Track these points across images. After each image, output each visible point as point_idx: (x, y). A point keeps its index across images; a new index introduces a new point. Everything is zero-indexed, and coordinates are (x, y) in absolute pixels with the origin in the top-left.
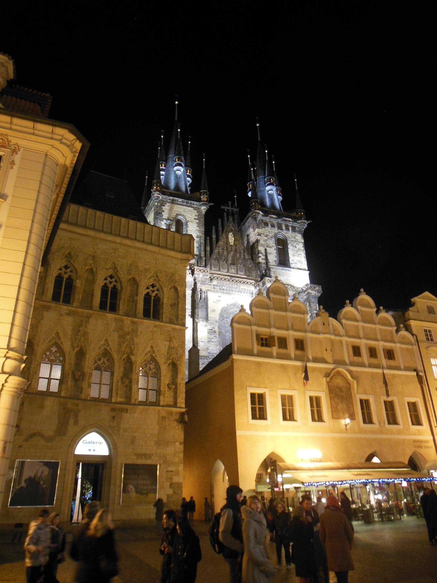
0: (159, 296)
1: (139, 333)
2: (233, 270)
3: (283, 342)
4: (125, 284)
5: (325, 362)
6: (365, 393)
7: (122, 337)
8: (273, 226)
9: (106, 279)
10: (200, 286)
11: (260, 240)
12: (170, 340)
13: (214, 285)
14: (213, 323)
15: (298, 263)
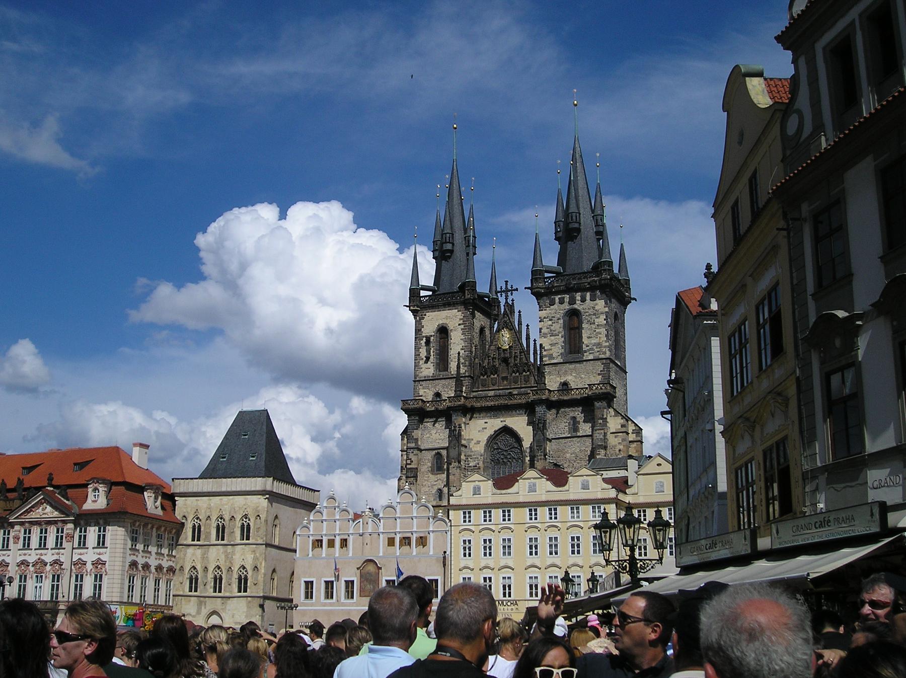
3: (331, 543)
7: (227, 556)
8: (562, 302)
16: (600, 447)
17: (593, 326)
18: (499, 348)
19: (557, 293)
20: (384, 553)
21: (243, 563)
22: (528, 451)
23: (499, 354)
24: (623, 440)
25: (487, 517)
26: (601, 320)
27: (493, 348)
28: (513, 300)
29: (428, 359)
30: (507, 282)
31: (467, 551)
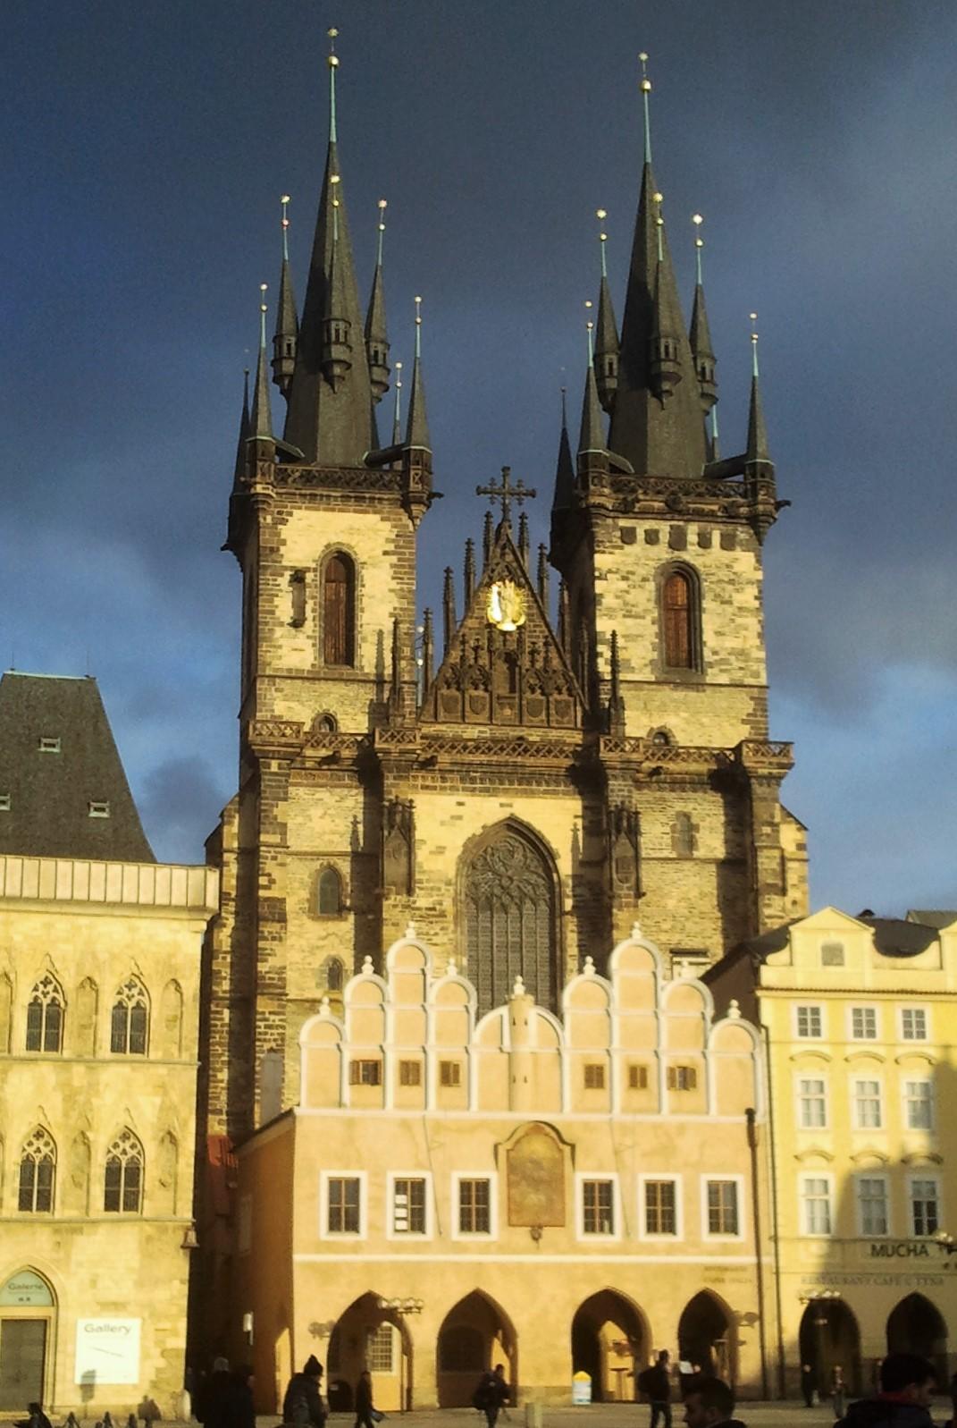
0: (142, 1005)
1: (101, 1088)
2: (508, 712)
3: (411, 1073)
4: (71, 997)
5: (511, 1108)
6: (600, 1168)
7: (70, 1098)
8: (652, 538)
9: (36, 989)
10: (393, 786)
11: (601, 595)
12: (166, 1093)
13: (440, 770)
14: (439, 889)
15: (733, 658)
16: (772, 888)
17: (729, 609)
18: (490, 626)
19: (646, 514)
20: (576, 1109)
21: (123, 1119)
22: (570, 882)
23: (490, 640)
24: (802, 879)
25: (865, 1025)
26: (748, 597)
27: (471, 623)
28: (522, 517)
29: (297, 623)
30: (506, 469)
31: (818, 1113)
